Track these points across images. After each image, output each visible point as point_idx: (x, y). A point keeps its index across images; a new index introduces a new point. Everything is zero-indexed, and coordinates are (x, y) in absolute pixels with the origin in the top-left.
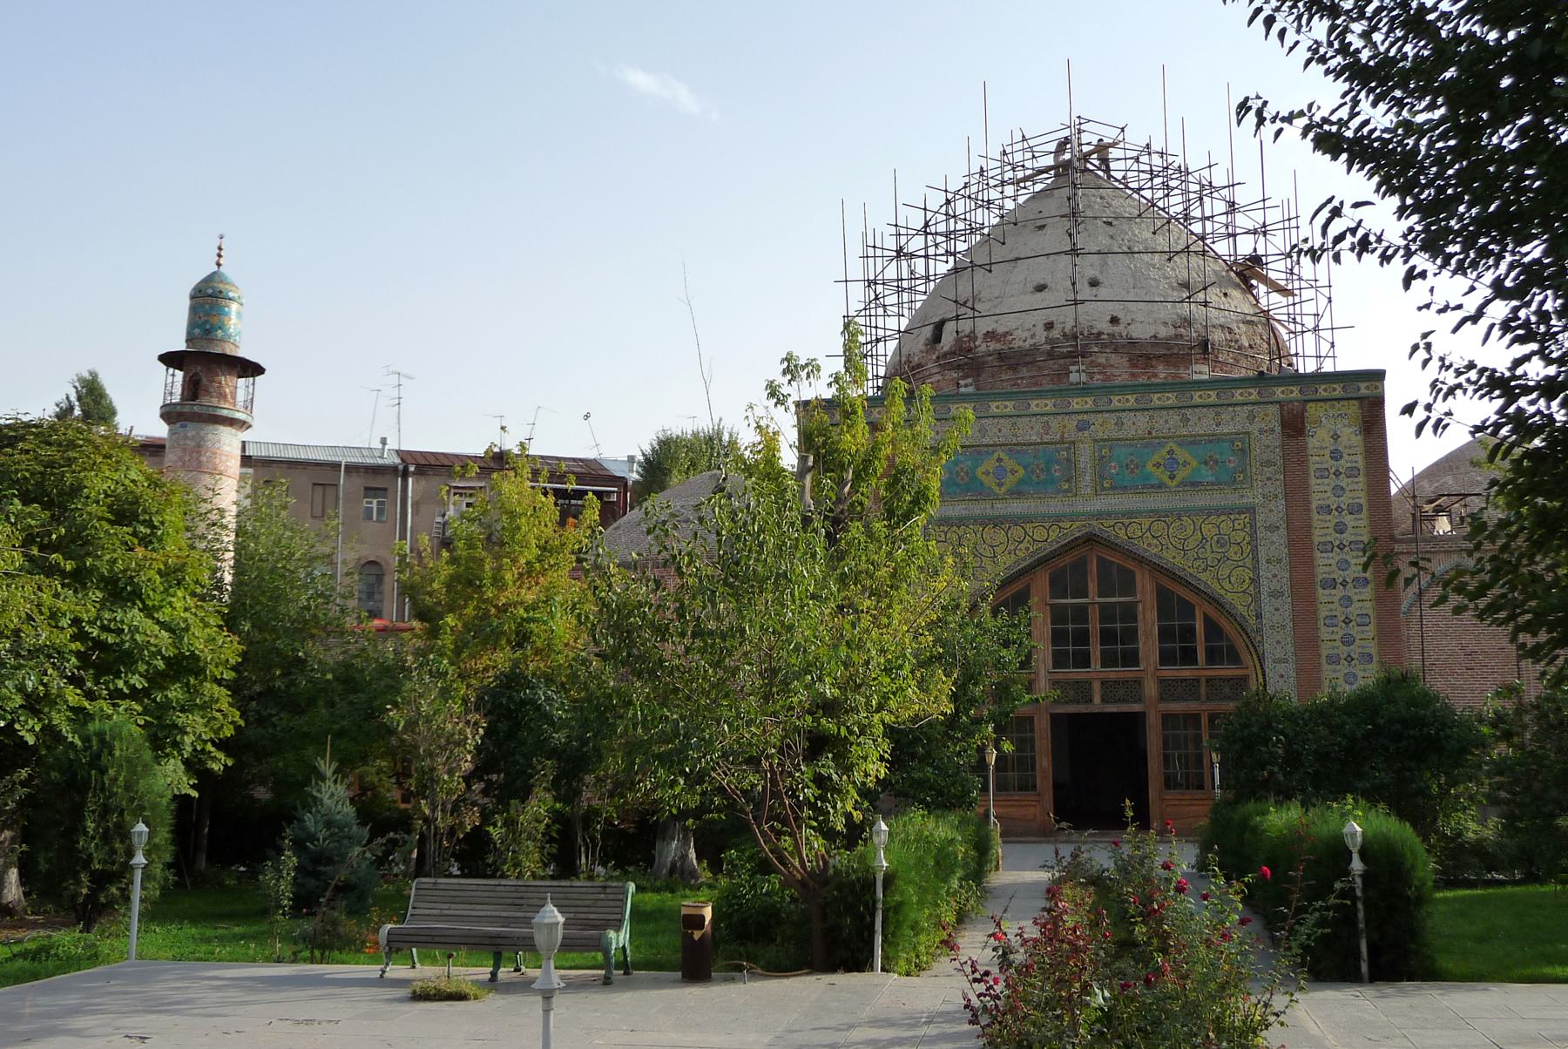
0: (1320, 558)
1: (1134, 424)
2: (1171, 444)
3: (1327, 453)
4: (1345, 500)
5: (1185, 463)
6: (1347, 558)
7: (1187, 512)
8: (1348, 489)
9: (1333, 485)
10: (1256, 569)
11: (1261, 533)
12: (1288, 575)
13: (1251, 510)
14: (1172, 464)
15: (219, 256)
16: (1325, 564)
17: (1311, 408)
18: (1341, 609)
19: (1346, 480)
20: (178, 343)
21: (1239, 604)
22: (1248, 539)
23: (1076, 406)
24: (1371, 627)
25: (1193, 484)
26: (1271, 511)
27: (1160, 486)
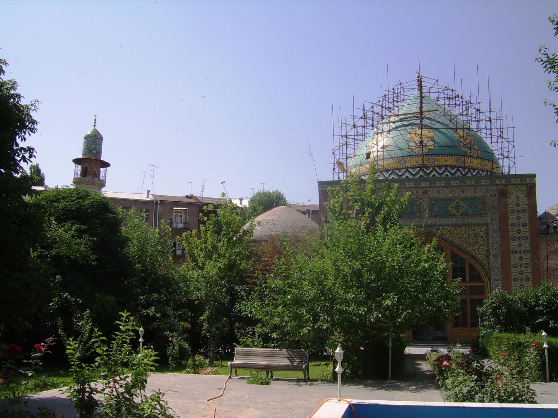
0: (512, 243)
1: (444, 192)
2: (458, 200)
3: (515, 204)
4: (521, 221)
5: (463, 207)
6: (521, 242)
7: (464, 225)
8: (522, 217)
9: (516, 215)
10: (488, 246)
11: (490, 233)
12: (500, 249)
13: (487, 225)
14: (458, 207)
15: (95, 123)
16: (514, 245)
17: (509, 188)
18: (518, 262)
19: (521, 214)
20: (80, 155)
21: (482, 259)
22: (485, 235)
23: (423, 185)
24: (530, 268)
25: (466, 215)
26: (494, 225)
27: (453, 215)
